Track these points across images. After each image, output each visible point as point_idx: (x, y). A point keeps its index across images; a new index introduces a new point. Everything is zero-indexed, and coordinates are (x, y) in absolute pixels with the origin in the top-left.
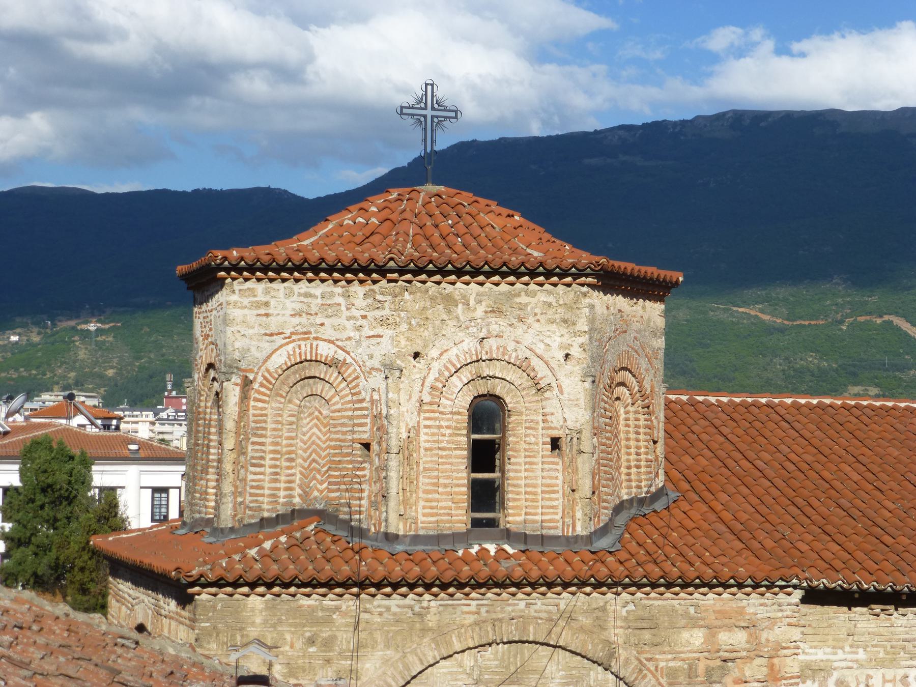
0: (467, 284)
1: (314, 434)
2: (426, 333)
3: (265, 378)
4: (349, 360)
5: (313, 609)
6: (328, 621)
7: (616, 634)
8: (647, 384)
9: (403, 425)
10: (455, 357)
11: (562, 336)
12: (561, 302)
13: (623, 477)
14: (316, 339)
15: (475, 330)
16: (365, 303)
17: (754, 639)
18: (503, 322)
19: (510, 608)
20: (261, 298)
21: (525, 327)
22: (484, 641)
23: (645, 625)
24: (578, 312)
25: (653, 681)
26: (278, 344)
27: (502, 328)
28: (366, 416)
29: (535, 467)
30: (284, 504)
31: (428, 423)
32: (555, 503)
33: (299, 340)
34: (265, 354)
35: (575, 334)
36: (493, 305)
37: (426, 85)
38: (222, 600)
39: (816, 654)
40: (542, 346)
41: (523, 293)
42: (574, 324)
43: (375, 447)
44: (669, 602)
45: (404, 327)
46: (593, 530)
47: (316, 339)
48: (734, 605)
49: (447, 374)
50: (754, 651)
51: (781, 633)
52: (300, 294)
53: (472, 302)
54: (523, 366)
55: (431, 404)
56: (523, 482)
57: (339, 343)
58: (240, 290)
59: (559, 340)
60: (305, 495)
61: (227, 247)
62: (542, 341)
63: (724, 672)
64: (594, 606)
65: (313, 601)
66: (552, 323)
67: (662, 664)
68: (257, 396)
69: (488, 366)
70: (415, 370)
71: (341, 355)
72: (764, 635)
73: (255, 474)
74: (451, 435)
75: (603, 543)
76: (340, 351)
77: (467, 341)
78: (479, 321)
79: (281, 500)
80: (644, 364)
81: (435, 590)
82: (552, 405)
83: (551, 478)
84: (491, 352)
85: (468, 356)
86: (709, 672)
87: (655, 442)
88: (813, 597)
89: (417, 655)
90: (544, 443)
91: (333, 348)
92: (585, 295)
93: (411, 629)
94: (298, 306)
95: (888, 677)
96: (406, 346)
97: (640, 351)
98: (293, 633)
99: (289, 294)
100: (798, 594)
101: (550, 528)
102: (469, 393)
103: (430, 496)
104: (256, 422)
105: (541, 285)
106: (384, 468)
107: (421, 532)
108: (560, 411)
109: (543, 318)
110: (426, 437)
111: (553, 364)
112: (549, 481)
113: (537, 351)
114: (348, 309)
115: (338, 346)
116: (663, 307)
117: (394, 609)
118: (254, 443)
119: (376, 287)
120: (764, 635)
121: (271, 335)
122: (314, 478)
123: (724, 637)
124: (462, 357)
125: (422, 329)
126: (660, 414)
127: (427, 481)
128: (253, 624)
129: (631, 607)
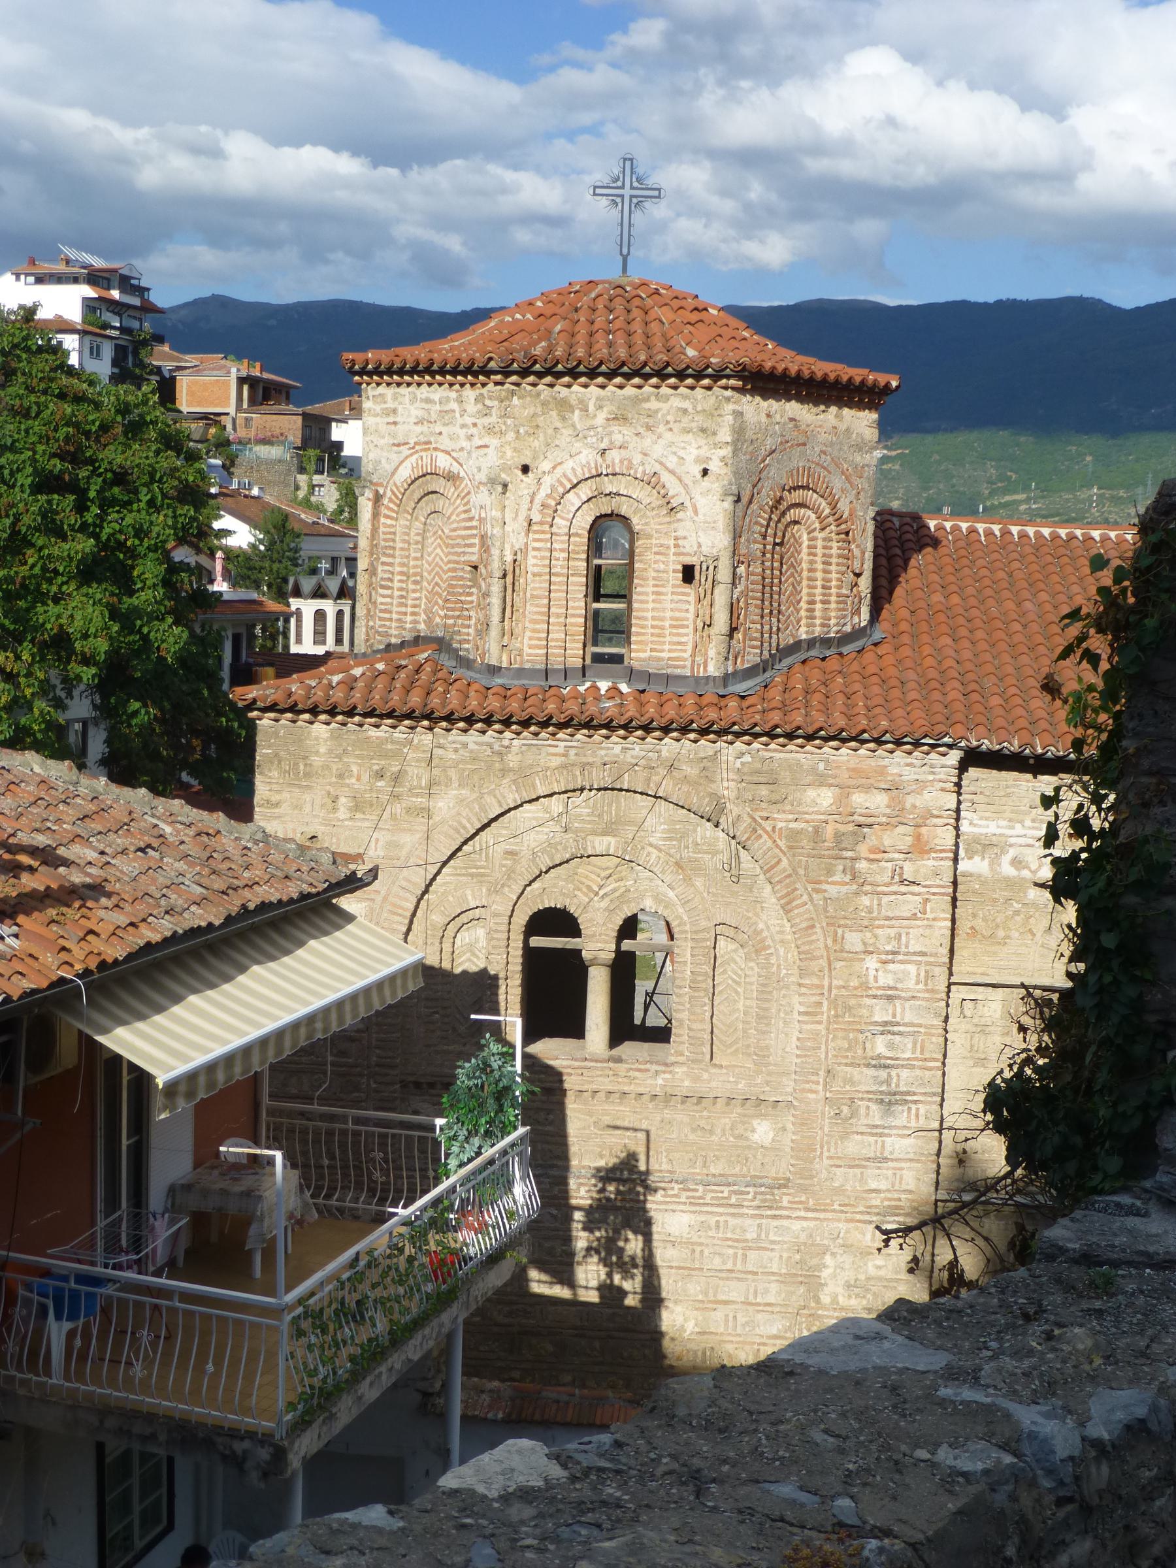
0: (586, 386)
2: (536, 443)
4: (462, 474)
5: (382, 741)
6: (397, 755)
7: (727, 787)
8: (844, 507)
9: (507, 547)
11: (699, 447)
12: (699, 408)
13: (803, 613)
14: (435, 449)
15: (594, 440)
16: (475, 410)
18: (628, 431)
19: (603, 752)
20: (390, 405)
21: (655, 437)
22: (571, 787)
23: (762, 780)
24: (720, 419)
25: (770, 843)
28: (474, 536)
29: (662, 597)
30: (411, 630)
31: (537, 545)
32: (683, 639)
33: (422, 450)
34: (394, 465)
37: (625, 160)
38: (284, 726)
39: (988, 826)
40: (675, 459)
41: (653, 398)
42: (714, 434)
43: (482, 569)
44: (793, 755)
45: (511, 436)
47: (435, 449)
48: (873, 762)
49: (561, 490)
50: (896, 818)
53: (591, 408)
54: (652, 481)
55: (541, 523)
56: (649, 615)
57: (454, 454)
59: (695, 452)
60: (428, 622)
61: (364, 349)
62: (675, 453)
64: (702, 755)
65: (383, 732)
67: (780, 825)
68: (386, 512)
69: (611, 482)
70: (523, 485)
71: (455, 468)
72: (910, 801)
73: (383, 596)
75: (741, 687)
76: (455, 464)
77: (585, 452)
78: (600, 429)
79: (408, 626)
80: (837, 483)
81: (533, 728)
82: (685, 525)
83: (680, 610)
84: (614, 465)
85: (586, 470)
86: (838, 836)
87: (858, 575)
89: (495, 797)
90: (674, 571)
92: (728, 399)
93: (489, 768)
94: (420, 413)
96: (513, 457)
97: (832, 468)
98: (359, 765)
99: (414, 399)
103: (538, 626)
104: (385, 540)
105: (675, 388)
106: (486, 595)
107: (527, 666)
109: (676, 427)
110: (535, 561)
111: (687, 480)
112: (677, 614)
113: (668, 465)
114: (462, 416)
116: (875, 416)
117: (471, 746)
118: (384, 564)
119: (484, 391)
120: (910, 801)
121: (399, 445)
122: (436, 603)
124: (579, 471)
127: (535, 609)
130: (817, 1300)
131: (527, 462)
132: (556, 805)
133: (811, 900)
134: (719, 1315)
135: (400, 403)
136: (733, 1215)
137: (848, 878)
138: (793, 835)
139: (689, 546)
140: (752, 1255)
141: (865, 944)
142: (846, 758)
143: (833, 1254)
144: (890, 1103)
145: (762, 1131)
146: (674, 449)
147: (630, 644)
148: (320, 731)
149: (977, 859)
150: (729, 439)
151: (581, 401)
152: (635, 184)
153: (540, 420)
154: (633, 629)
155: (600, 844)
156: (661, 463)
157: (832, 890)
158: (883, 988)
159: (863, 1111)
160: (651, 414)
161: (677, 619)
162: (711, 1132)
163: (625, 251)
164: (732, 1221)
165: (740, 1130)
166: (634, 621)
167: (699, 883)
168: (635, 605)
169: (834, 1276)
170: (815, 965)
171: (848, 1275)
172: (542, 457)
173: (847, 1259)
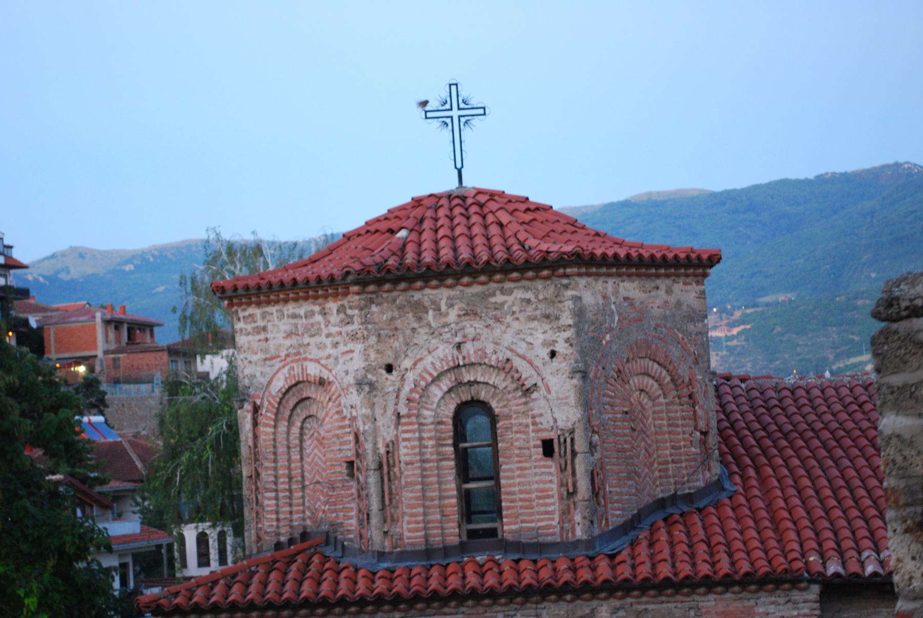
1: (316, 455)
2: (397, 344)
3: (270, 403)
4: (331, 379)
8: (683, 371)
10: (430, 365)
11: (545, 332)
12: (541, 297)
14: (305, 359)
15: (449, 335)
16: (338, 320)
18: (478, 324)
20: (261, 323)
21: (503, 328)
24: (560, 305)
26: (276, 368)
27: (478, 330)
29: (527, 472)
31: (406, 436)
32: (550, 509)
33: (292, 362)
34: (268, 378)
35: (560, 329)
36: (466, 308)
40: (524, 345)
41: (498, 292)
42: (557, 318)
43: (357, 463)
44: (664, 605)
45: (373, 339)
46: (597, 532)
48: (739, 604)
49: (423, 383)
52: (288, 316)
53: (443, 308)
54: (506, 367)
55: (408, 416)
56: (516, 489)
57: (323, 362)
58: (244, 317)
60: (313, 517)
62: (524, 340)
66: (533, 320)
68: (264, 421)
69: (468, 372)
70: (388, 383)
71: (325, 374)
74: (433, 447)
77: (441, 347)
78: (453, 326)
80: (675, 352)
82: (539, 403)
83: (545, 482)
84: (469, 356)
85: (444, 363)
90: (535, 447)
91: (319, 367)
92: (566, 287)
96: (376, 359)
99: (282, 316)
100: (816, 589)
101: (547, 535)
102: (452, 401)
103: (414, 511)
107: (409, 548)
108: (550, 411)
109: (522, 317)
111: (538, 363)
112: (541, 486)
114: (326, 326)
115: (323, 365)
121: (272, 358)
122: (319, 500)
124: (438, 365)
125: (392, 340)
127: (411, 495)
131: (390, 361)
135: (269, 321)
139: (546, 422)
142: (713, 603)
146: (522, 336)
147: (501, 517)
150: (570, 322)
151: (433, 302)
152: (462, 106)
153: (398, 323)
154: (503, 504)
156: (512, 350)
160: (498, 307)
161: (543, 491)
163: (459, 166)
166: (503, 497)
168: (503, 482)
172: (403, 356)
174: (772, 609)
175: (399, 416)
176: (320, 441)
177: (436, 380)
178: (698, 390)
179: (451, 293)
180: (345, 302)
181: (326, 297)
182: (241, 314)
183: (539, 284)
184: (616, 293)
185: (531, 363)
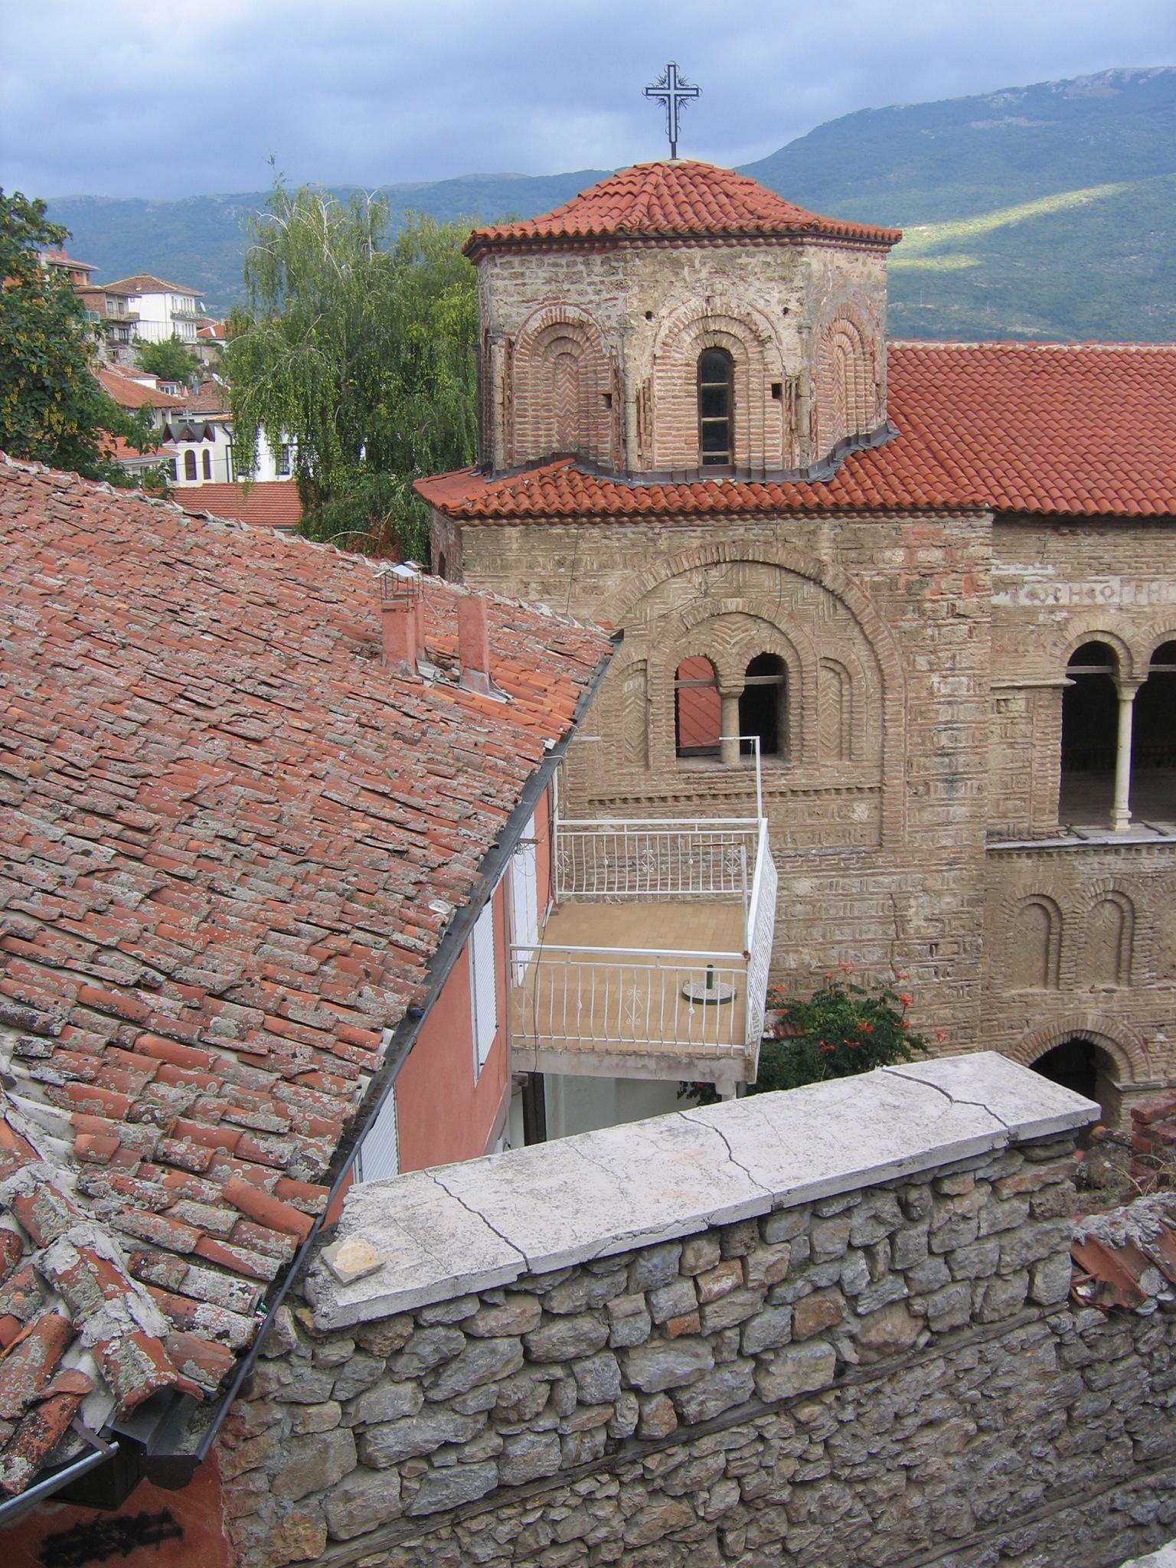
2: (656, 295)
4: (592, 321)
5: (560, 536)
7: (826, 552)
8: (868, 332)
9: (638, 377)
14: (564, 303)
17: (950, 558)
25: (859, 594)
26: (531, 311)
35: (793, 290)
40: (762, 302)
42: (791, 281)
43: (614, 397)
45: (636, 289)
46: (810, 463)
48: (931, 527)
51: (978, 550)
53: (697, 265)
54: (744, 321)
55: (662, 358)
60: (562, 440)
63: (923, 584)
71: (585, 317)
72: (959, 553)
73: (521, 423)
80: (865, 315)
82: (771, 354)
86: (909, 587)
88: (1007, 518)
92: (801, 254)
94: (547, 275)
95: (1075, 590)
99: (539, 267)
100: (990, 517)
109: (762, 277)
111: (773, 318)
115: (583, 310)
117: (630, 535)
123: (922, 555)
126: (882, 359)
128: (510, 550)
129: (838, 530)
130: (904, 931)
132: (697, 578)
133: (891, 635)
134: (834, 953)
136: (843, 876)
137: (916, 616)
138: (876, 587)
140: (857, 904)
141: (930, 663)
143: (916, 898)
144: (952, 781)
145: (861, 811)
148: (512, 533)
149: (1002, 594)
150: (802, 284)
154: (737, 436)
155: (733, 604)
157: (905, 625)
158: (944, 696)
159: (932, 789)
160: (743, 267)
162: (824, 816)
164: (841, 881)
165: (844, 812)
167: (807, 628)
168: (738, 418)
169: (917, 913)
170: (895, 683)
171: (927, 912)
173: (924, 899)
174: (956, 531)
175: (655, 357)
176: (575, 376)
177: (687, 327)
178: (877, 348)
179: (704, 252)
180: (610, 255)
181: (592, 250)
182: (498, 261)
183: (777, 250)
184: (832, 262)
185: (767, 318)
